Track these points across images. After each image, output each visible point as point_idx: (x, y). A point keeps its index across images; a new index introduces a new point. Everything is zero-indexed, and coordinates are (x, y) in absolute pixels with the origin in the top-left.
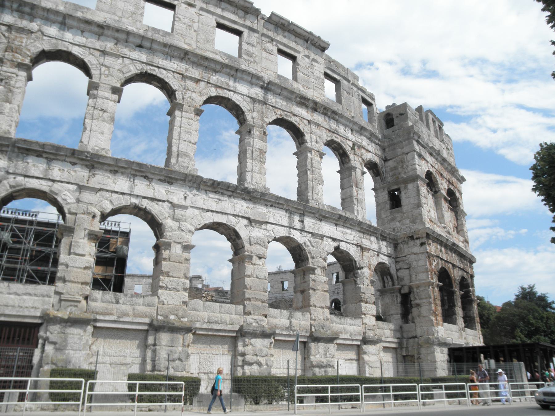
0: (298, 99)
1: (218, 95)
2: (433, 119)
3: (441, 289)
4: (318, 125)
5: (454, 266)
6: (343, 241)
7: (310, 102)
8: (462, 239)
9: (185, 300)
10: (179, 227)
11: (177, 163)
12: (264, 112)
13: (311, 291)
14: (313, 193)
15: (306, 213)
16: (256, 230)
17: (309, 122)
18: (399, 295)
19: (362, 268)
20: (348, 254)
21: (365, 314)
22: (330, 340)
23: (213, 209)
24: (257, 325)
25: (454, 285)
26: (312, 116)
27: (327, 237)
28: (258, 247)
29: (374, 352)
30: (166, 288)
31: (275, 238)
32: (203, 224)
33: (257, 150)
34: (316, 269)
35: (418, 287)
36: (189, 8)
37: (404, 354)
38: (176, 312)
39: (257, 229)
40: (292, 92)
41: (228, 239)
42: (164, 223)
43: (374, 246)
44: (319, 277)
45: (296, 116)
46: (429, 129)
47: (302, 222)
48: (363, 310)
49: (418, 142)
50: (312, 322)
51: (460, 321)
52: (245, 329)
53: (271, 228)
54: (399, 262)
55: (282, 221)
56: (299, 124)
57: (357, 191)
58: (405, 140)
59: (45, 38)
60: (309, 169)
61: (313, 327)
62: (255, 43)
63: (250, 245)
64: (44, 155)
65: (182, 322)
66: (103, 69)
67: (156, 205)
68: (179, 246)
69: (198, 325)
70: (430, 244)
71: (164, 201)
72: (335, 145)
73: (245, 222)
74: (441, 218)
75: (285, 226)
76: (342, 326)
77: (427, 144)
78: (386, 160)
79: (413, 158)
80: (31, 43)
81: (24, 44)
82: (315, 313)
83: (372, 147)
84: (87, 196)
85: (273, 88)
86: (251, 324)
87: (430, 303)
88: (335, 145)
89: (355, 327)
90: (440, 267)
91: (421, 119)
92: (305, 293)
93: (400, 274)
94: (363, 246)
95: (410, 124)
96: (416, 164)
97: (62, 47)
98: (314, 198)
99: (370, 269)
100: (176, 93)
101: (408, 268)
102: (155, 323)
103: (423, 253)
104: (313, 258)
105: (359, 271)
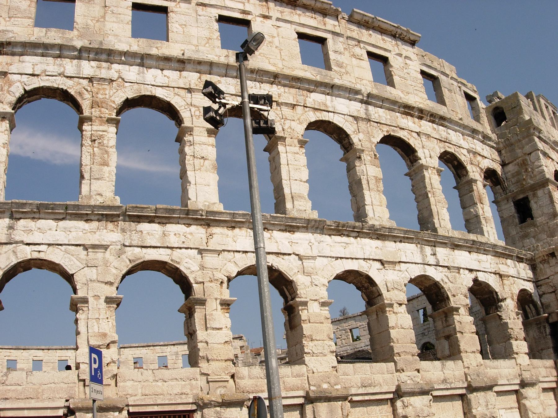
0: (402, 109)
1: (318, 119)
2: (545, 104)
4: (428, 136)
6: (480, 271)
7: (415, 110)
9: (334, 365)
11: (293, 207)
12: (370, 130)
13: (458, 335)
14: (439, 219)
15: (437, 245)
16: (390, 272)
17: (418, 134)
18: (547, 325)
19: (505, 299)
20: (487, 286)
21: (517, 354)
22: (489, 388)
23: (342, 256)
26: (420, 126)
27: (463, 269)
28: (396, 291)
31: (411, 279)
32: (335, 275)
33: (373, 178)
34: (459, 308)
36: (265, 21)
38: (328, 380)
39: (392, 271)
40: (394, 102)
41: (358, 288)
42: (294, 280)
43: (512, 271)
44: (464, 317)
45: (403, 129)
46: (545, 118)
48: (515, 349)
49: (539, 138)
50: (466, 370)
52: (404, 388)
54: (541, 285)
57: (483, 209)
58: (524, 138)
59: (127, 84)
60: (429, 191)
61: (468, 376)
62: (342, 50)
63: (388, 291)
64: (156, 220)
65: (337, 390)
66: (193, 109)
68: (316, 304)
69: (353, 391)
71: (290, 254)
72: (448, 156)
73: (378, 265)
75: (418, 264)
76: (496, 371)
77: (549, 138)
78: (504, 165)
79: (539, 159)
80: (115, 93)
81: (107, 97)
82: (468, 360)
83: (486, 151)
84: (210, 260)
88: (448, 156)
89: (510, 370)
91: (535, 109)
92: (451, 338)
93: (545, 299)
94: (501, 273)
95: (527, 118)
96: (542, 165)
97: (147, 91)
98: (442, 224)
99: (513, 299)
102: (312, 395)
104: (454, 296)
105: (502, 303)
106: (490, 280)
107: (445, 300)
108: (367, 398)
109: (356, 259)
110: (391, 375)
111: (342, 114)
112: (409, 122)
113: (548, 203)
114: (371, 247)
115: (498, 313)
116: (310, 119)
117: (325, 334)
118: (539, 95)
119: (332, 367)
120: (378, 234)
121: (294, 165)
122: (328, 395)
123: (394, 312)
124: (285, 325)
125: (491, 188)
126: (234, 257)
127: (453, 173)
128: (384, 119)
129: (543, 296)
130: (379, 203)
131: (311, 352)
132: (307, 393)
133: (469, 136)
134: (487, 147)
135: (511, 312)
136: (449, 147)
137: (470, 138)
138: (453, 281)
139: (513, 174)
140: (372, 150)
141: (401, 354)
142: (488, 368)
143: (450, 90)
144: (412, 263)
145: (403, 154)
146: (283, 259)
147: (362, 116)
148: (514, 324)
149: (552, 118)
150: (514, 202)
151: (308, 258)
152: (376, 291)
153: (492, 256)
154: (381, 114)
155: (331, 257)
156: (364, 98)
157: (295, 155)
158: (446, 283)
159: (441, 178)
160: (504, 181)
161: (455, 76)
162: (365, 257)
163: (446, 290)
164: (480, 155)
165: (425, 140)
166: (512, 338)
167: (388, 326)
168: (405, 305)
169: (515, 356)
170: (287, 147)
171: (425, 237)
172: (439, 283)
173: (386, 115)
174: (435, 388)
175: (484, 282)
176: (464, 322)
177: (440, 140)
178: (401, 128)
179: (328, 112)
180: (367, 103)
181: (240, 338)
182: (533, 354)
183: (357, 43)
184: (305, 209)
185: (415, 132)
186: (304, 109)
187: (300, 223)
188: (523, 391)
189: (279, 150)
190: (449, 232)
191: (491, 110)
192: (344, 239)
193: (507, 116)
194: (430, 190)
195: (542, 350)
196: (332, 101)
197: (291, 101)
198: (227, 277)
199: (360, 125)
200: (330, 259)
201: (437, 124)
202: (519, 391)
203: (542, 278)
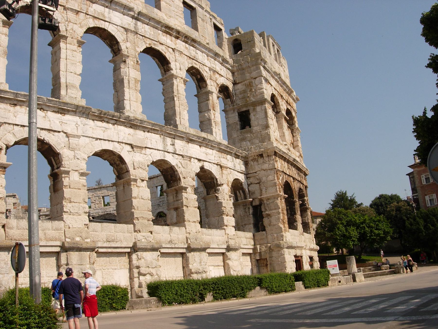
0: (163, 28)
1: (95, 26)
2: (273, 43)
3: (287, 200)
4: (181, 53)
5: (294, 179)
6: (207, 161)
7: (173, 31)
8: (298, 154)
9: (87, 223)
10: (74, 156)
11: (67, 94)
12: (136, 41)
13: (185, 208)
14: (180, 118)
15: (176, 137)
16: (137, 154)
17: (173, 50)
18: (251, 207)
19: (223, 184)
20: (210, 173)
21: (227, 226)
22: (203, 250)
23: (101, 138)
25: (295, 196)
26: (176, 44)
27: (194, 158)
28: (140, 170)
29: (236, 258)
30: (70, 213)
31: (153, 161)
32: (94, 152)
33: (133, 79)
34: (187, 188)
35: (268, 199)
37: (258, 258)
40: (159, 22)
41: (111, 164)
42: (61, 152)
43: (230, 165)
45: (162, 44)
48: (225, 222)
49: (264, 67)
50: (188, 235)
51: (300, 226)
52: (139, 245)
53: (149, 153)
54: (250, 177)
55: (158, 145)
56: (165, 53)
57: (214, 115)
58: (253, 66)
60: (175, 96)
61: (189, 240)
65: (87, 243)
67: (53, 136)
68: (77, 173)
69: (100, 245)
70: (277, 161)
71: (59, 132)
72: (194, 71)
73: (129, 148)
74: (283, 136)
75: (160, 150)
76: (210, 237)
78: (235, 83)
79: (261, 83)
82: (190, 227)
83: (224, 71)
87: (279, 213)
88: (194, 71)
89: (220, 237)
90: (285, 181)
91: (265, 45)
93: (252, 188)
94: (222, 165)
95: (257, 51)
96: (263, 88)
98: (182, 122)
99: (228, 185)
101: (259, 183)
102: (66, 245)
103: (272, 169)
104: (184, 178)
105: (220, 187)
106: (213, 169)
107: (177, 181)
108: (110, 250)
109: (112, 141)
110: (130, 234)
111: (116, 25)
112: (167, 40)
113: (263, 117)
114: (125, 133)
116: (89, 25)
117: (81, 198)
118: (269, 36)
119: (85, 225)
120: (131, 124)
121: (71, 60)
122: (79, 246)
123: (137, 186)
124: (50, 188)
125: (223, 100)
126: (14, 129)
129: (251, 185)
130: (135, 100)
131: (69, 211)
132: (63, 243)
133: (212, 57)
135: (225, 195)
136: (195, 64)
137: (213, 60)
138: (185, 167)
139: (240, 92)
140: (135, 57)
141: (139, 219)
142: (204, 235)
143: (203, 20)
144: (155, 149)
145: (160, 64)
146: (53, 135)
147: (131, 29)
149: (276, 54)
150: (238, 113)
151: (74, 136)
152: (125, 168)
153: (217, 151)
154: (146, 30)
155: (92, 138)
156: (135, 14)
157: (74, 52)
158: (179, 167)
159: (186, 87)
160: (233, 96)
161: (209, 10)
162: (120, 141)
163: (179, 173)
164: (218, 73)
165: (178, 55)
166: (224, 214)
167: (131, 196)
168: (146, 181)
169: (225, 227)
170: (68, 45)
171: (167, 131)
172: (174, 167)
173: (151, 31)
174: (163, 246)
175: (208, 170)
176: (190, 199)
177: (189, 57)
178: (160, 43)
179: (105, 21)
180: (137, 19)
181: (14, 197)
182: (239, 227)
184: (76, 96)
185: (171, 48)
186: (86, 16)
188: (228, 254)
189: (61, 46)
190: (187, 129)
191: (232, 40)
192: (105, 124)
193: (243, 47)
195: (245, 225)
196: (109, 13)
197: (76, 8)
198: (6, 145)
199: (129, 36)
200: (91, 139)
201: (189, 45)
202: (225, 254)
203: (251, 172)
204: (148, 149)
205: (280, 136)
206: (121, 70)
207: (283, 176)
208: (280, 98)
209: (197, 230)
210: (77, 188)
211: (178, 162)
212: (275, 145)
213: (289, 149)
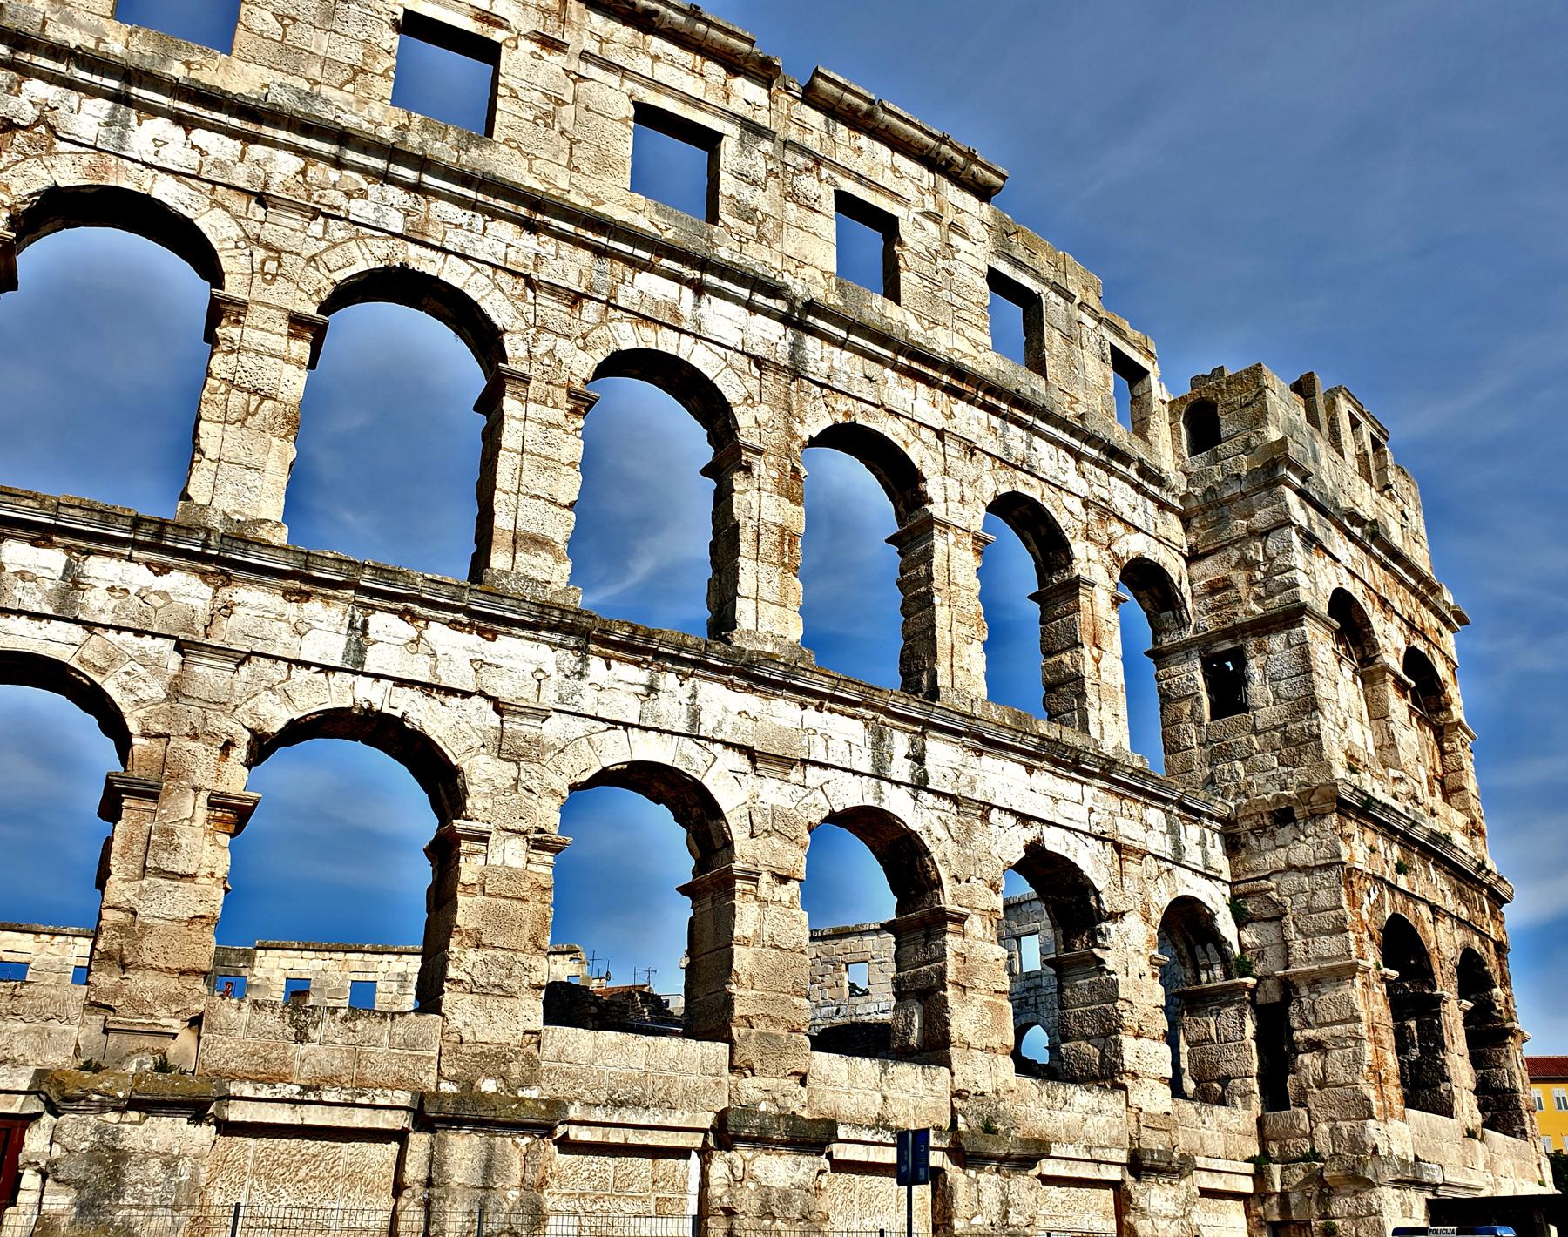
1: (642, 345)
5: (1434, 909)
8: (1460, 819)
9: (531, 1027)
13: (951, 993)
17: (940, 434)
19: (1123, 914)
21: (1135, 1075)
24: (773, 1110)
26: (951, 416)
27: (1001, 809)
28: (776, 842)
31: (832, 812)
34: (967, 916)
38: (503, 1068)
40: (883, 339)
42: (464, 767)
43: (1159, 843)
45: (898, 415)
47: (918, 758)
48: (1129, 1061)
49: (1301, 493)
57: (1097, 661)
59: (61, 146)
60: (939, 590)
61: (960, 1119)
65: (521, 1101)
69: (574, 1112)
70: (1350, 836)
71: (466, 695)
74: (1388, 745)
75: (862, 774)
79: (1288, 549)
82: (969, 1070)
84: (209, 675)
85: (821, 324)
86: (756, 1104)
88: (1023, 509)
90: (1388, 914)
91: (1312, 418)
92: (932, 998)
94: (1119, 840)
97: (126, 178)
98: (957, 682)
100: (506, 337)
108: (616, 1137)
110: (711, 1078)
112: (922, 403)
115: (1095, 950)
116: (619, 341)
117: (527, 931)
118: (1338, 389)
121: (539, 455)
127: (1035, 558)
128: (844, 378)
131: (468, 979)
133: (1096, 463)
134: (1149, 503)
138: (961, 839)
139: (1210, 585)
141: (754, 1021)
143: (1068, 338)
144: (845, 770)
146: (443, 704)
148: (1138, 988)
149: (1366, 454)
151: (523, 712)
154: (836, 365)
157: (551, 429)
159: (984, 561)
160: (1183, 599)
161: (1093, 302)
164: (1120, 519)
165: (955, 453)
167: (732, 933)
168: (797, 883)
169: (1128, 1081)
170: (531, 406)
171: (893, 706)
177: (1002, 460)
178: (890, 411)
179: (681, 331)
183: (811, 164)
185: (931, 428)
187: (516, 612)
189: (505, 408)
190: (976, 706)
194: (941, 587)
196: (697, 306)
197: (572, 282)
198: (251, 731)
199: (768, 383)
204: (816, 770)
205: (1378, 748)
206: (735, 499)
207: (1381, 895)
208: (1377, 606)
209: (1000, 1081)
210: (510, 895)
211: (935, 820)
212: (1340, 772)
213: (1415, 798)
